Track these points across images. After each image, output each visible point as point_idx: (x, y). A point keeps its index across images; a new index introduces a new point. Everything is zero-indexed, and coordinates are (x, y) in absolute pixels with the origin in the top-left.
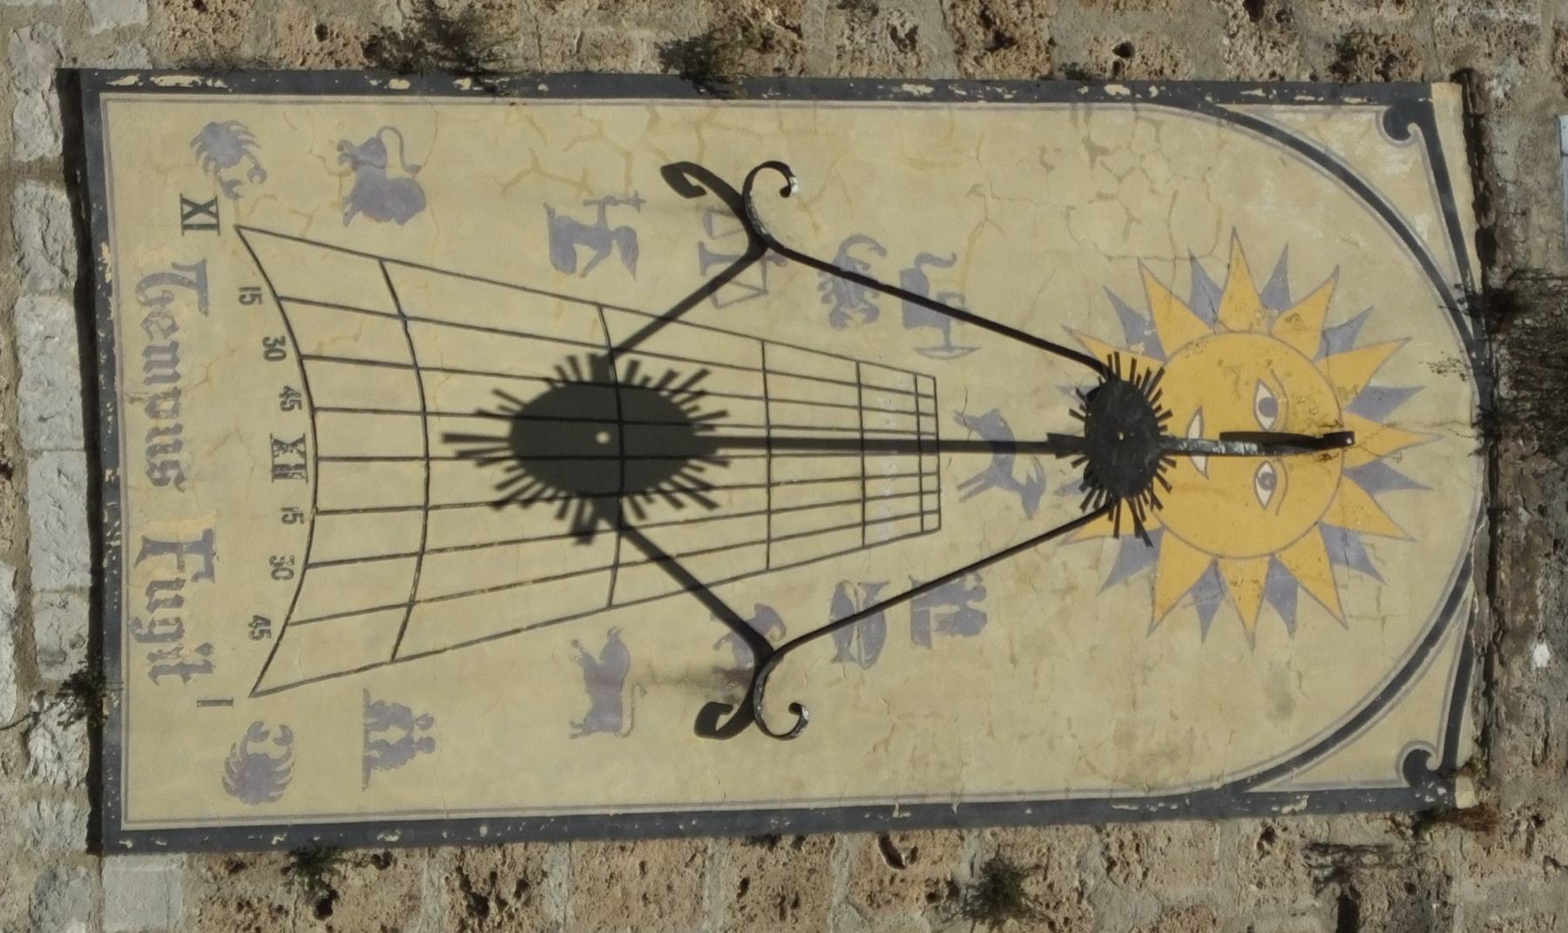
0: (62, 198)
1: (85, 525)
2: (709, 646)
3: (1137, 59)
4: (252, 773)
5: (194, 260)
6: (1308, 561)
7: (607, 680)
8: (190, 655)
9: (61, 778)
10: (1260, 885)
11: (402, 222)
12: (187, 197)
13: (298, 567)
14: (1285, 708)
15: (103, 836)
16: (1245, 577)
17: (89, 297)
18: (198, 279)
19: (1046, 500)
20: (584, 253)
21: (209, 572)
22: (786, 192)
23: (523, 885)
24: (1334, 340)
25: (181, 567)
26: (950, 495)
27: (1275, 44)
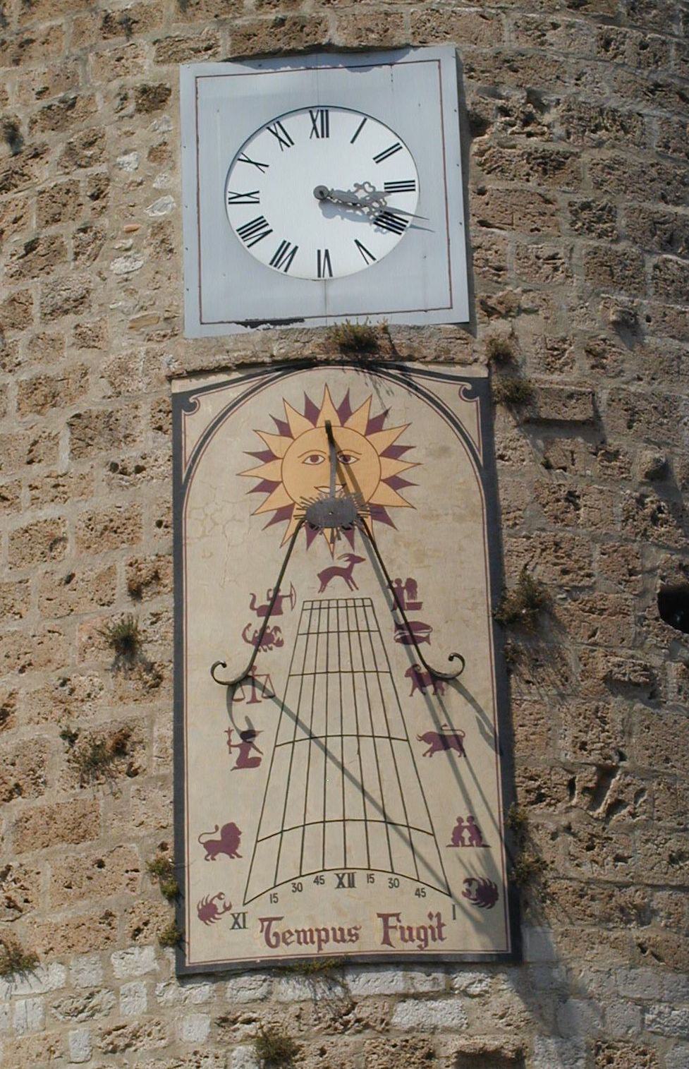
0: (231, 983)
1: (378, 971)
3: (163, 518)
5: (259, 922)
6: (382, 440)
8: (434, 923)
9: (489, 980)
10: (523, 460)
11: (240, 833)
12: (231, 926)
13: (394, 876)
14: (445, 451)
16: (391, 467)
19: (357, 554)
20: (252, 754)
21: (397, 915)
22: (224, 665)
23: (531, 778)
24: (284, 430)
25: (395, 927)
26: (356, 594)
27: (156, 460)
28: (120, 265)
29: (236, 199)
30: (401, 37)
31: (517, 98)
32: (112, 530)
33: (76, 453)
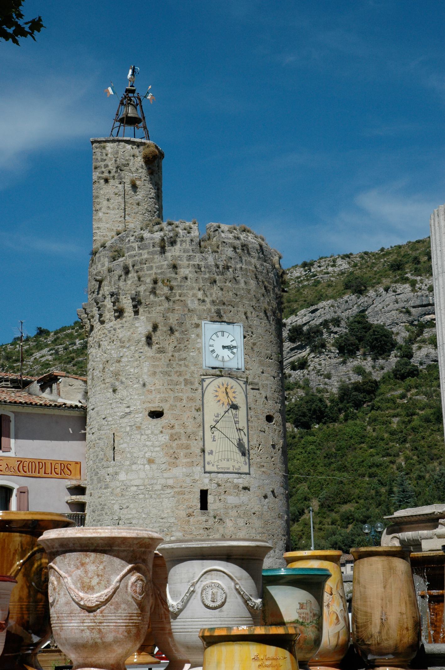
6: (233, 390)
15: (250, 474)
17: (218, 473)
18: (217, 465)
28: (191, 354)
29: (210, 346)
30: (235, 321)
31: (250, 333)
32: (192, 399)
33: (185, 386)
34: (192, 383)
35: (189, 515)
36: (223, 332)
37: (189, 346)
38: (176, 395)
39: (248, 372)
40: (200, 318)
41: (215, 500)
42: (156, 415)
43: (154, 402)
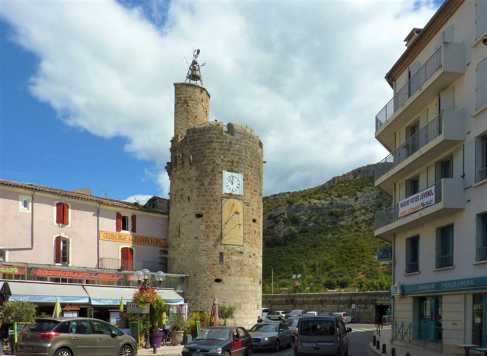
2: (238, 226)
4: (242, 241)
7: (240, 230)
17: (228, 245)
18: (228, 241)
28: (217, 186)
31: (247, 178)
34: (217, 201)
35: (214, 264)
36: (233, 176)
37: (216, 182)
38: (209, 206)
39: (245, 197)
40: (222, 169)
41: (226, 257)
42: (199, 216)
43: (198, 210)
